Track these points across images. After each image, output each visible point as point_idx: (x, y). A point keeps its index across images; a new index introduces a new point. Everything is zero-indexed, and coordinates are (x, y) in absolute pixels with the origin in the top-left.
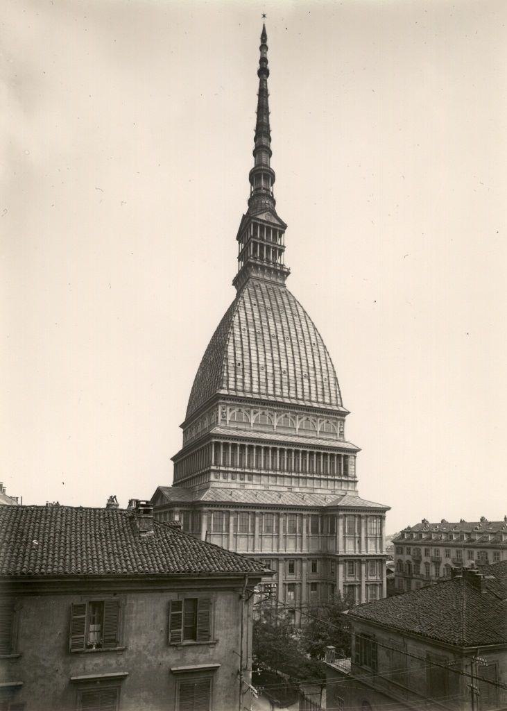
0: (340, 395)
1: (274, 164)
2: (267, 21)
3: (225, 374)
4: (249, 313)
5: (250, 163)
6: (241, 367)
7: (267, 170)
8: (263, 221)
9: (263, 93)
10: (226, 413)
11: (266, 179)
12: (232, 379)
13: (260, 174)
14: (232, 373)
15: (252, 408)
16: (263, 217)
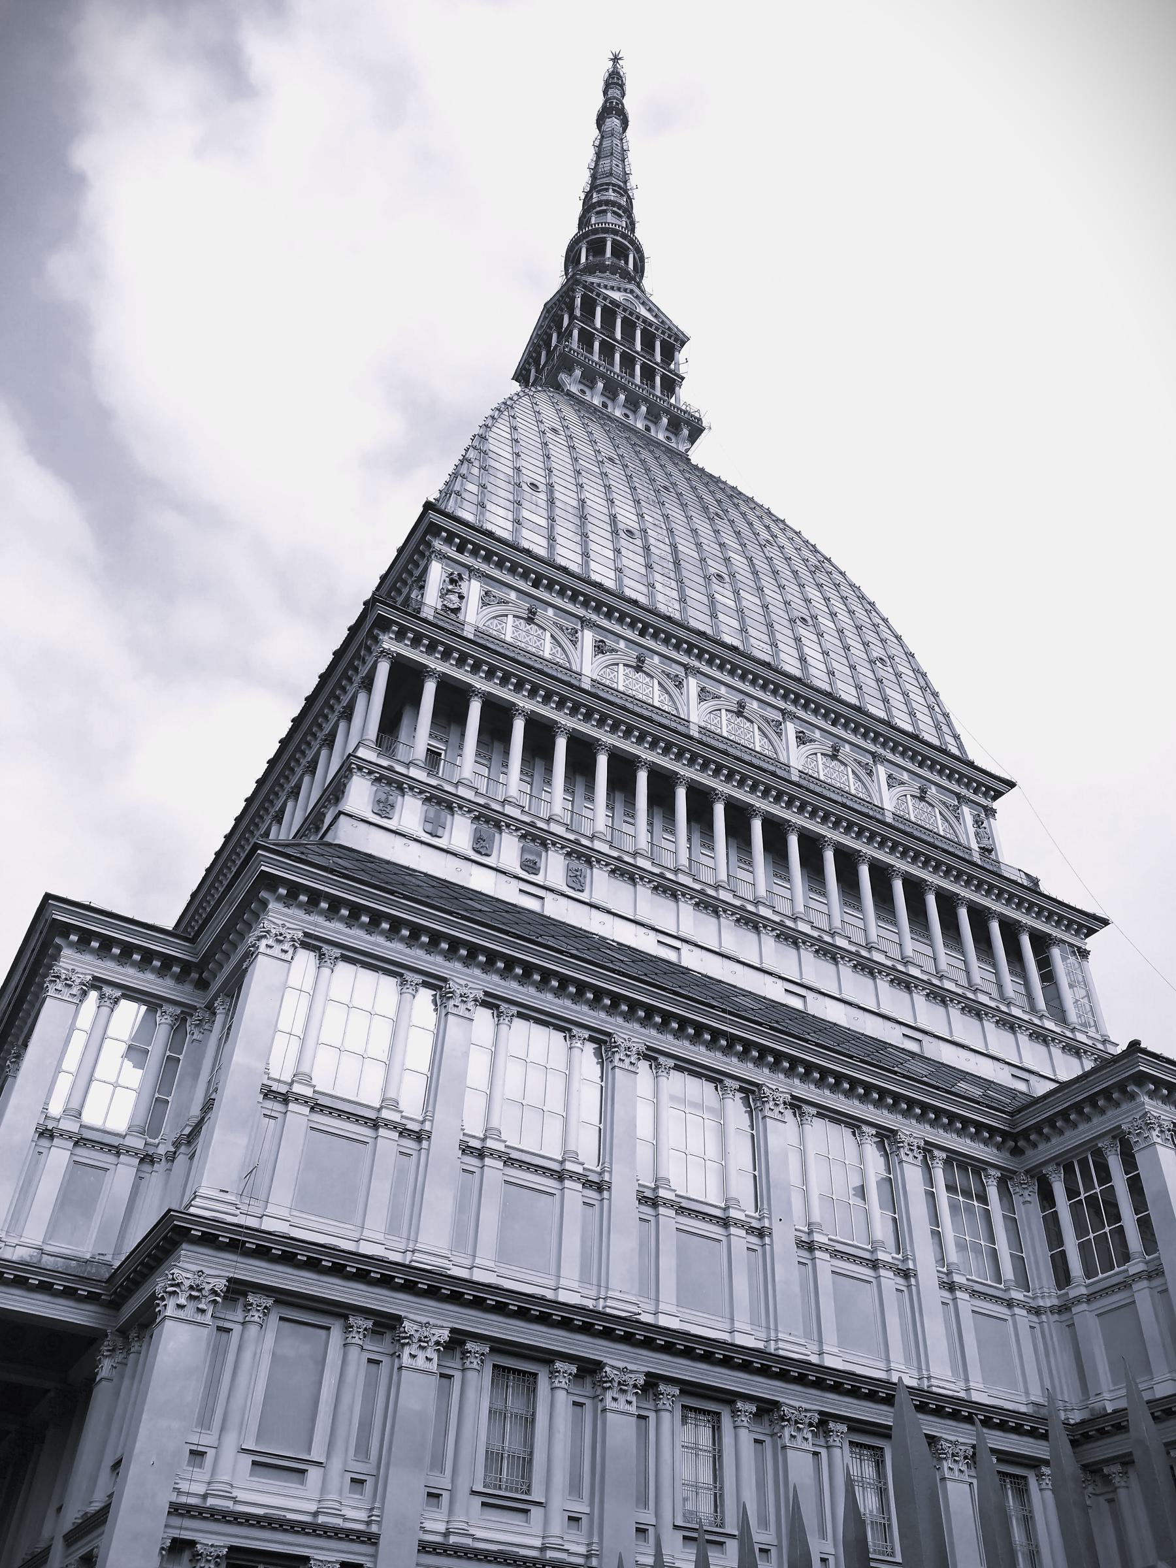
0: (950, 725)
3: (473, 488)
6: (543, 496)
7: (624, 236)
8: (613, 302)
13: (604, 240)
14: (501, 492)
16: (617, 296)
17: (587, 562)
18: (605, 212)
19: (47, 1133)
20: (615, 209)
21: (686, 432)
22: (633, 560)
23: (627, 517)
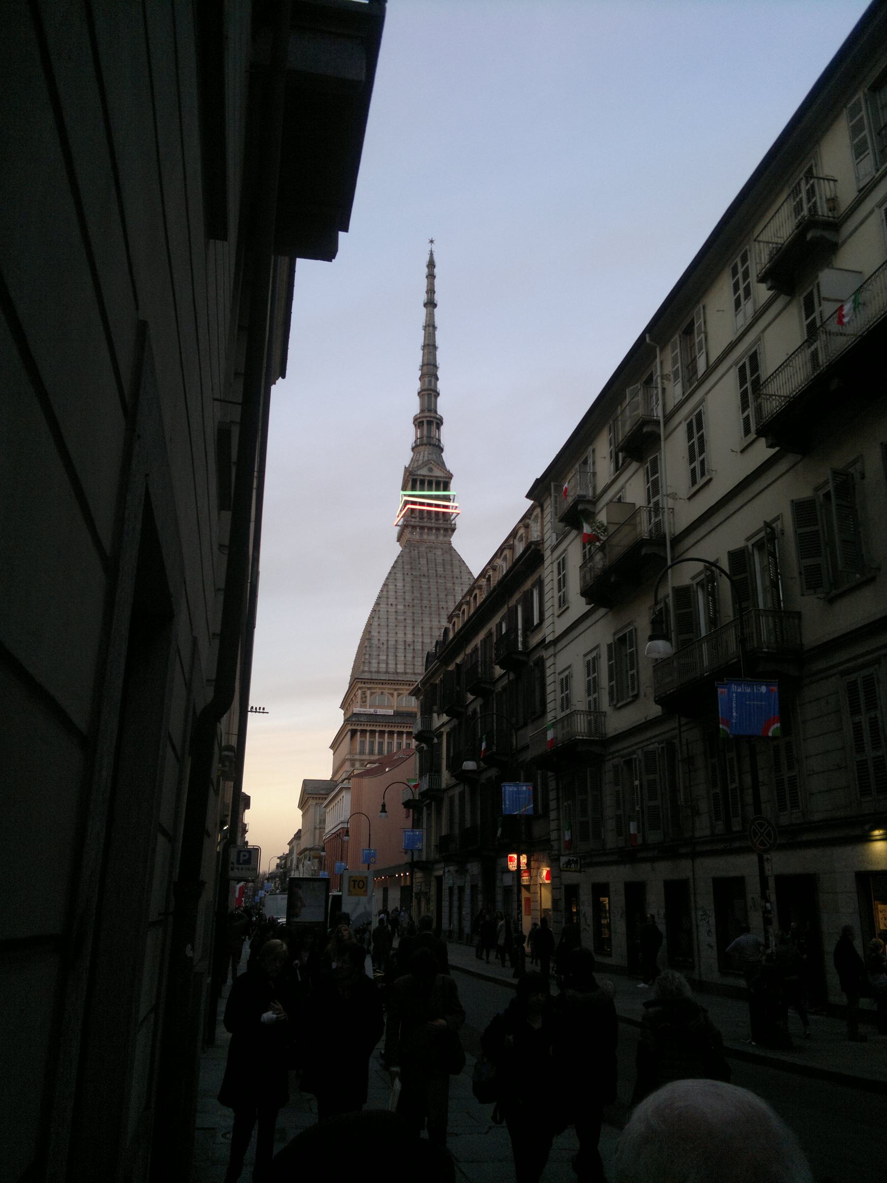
1: (443, 406)
2: (435, 248)
3: (367, 657)
4: (400, 584)
5: (414, 406)
6: (385, 647)
7: (430, 417)
8: (424, 476)
9: (430, 327)
10: (366, 697)
11: (430, 423)
12: (374, 661)
13: (422, 422)
15: (396, 690)
16: (424, 472)
17: (396, 667)
18: (424, 394)
19: (315, 828)
20: (429, 392)
21: (450, 532)
22: (409, 656)
23: (409, 638)
